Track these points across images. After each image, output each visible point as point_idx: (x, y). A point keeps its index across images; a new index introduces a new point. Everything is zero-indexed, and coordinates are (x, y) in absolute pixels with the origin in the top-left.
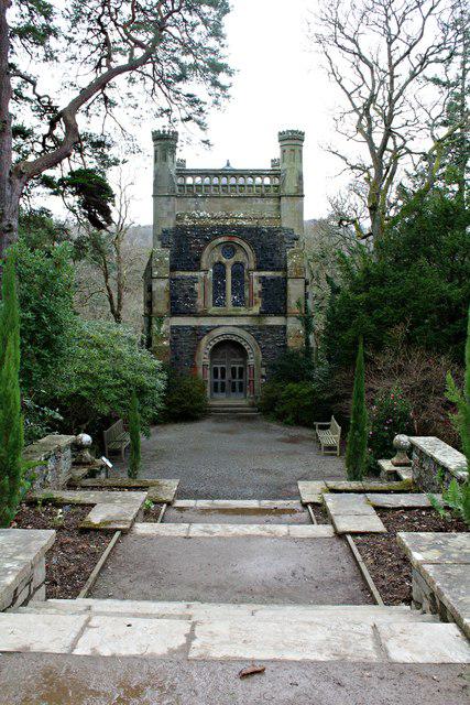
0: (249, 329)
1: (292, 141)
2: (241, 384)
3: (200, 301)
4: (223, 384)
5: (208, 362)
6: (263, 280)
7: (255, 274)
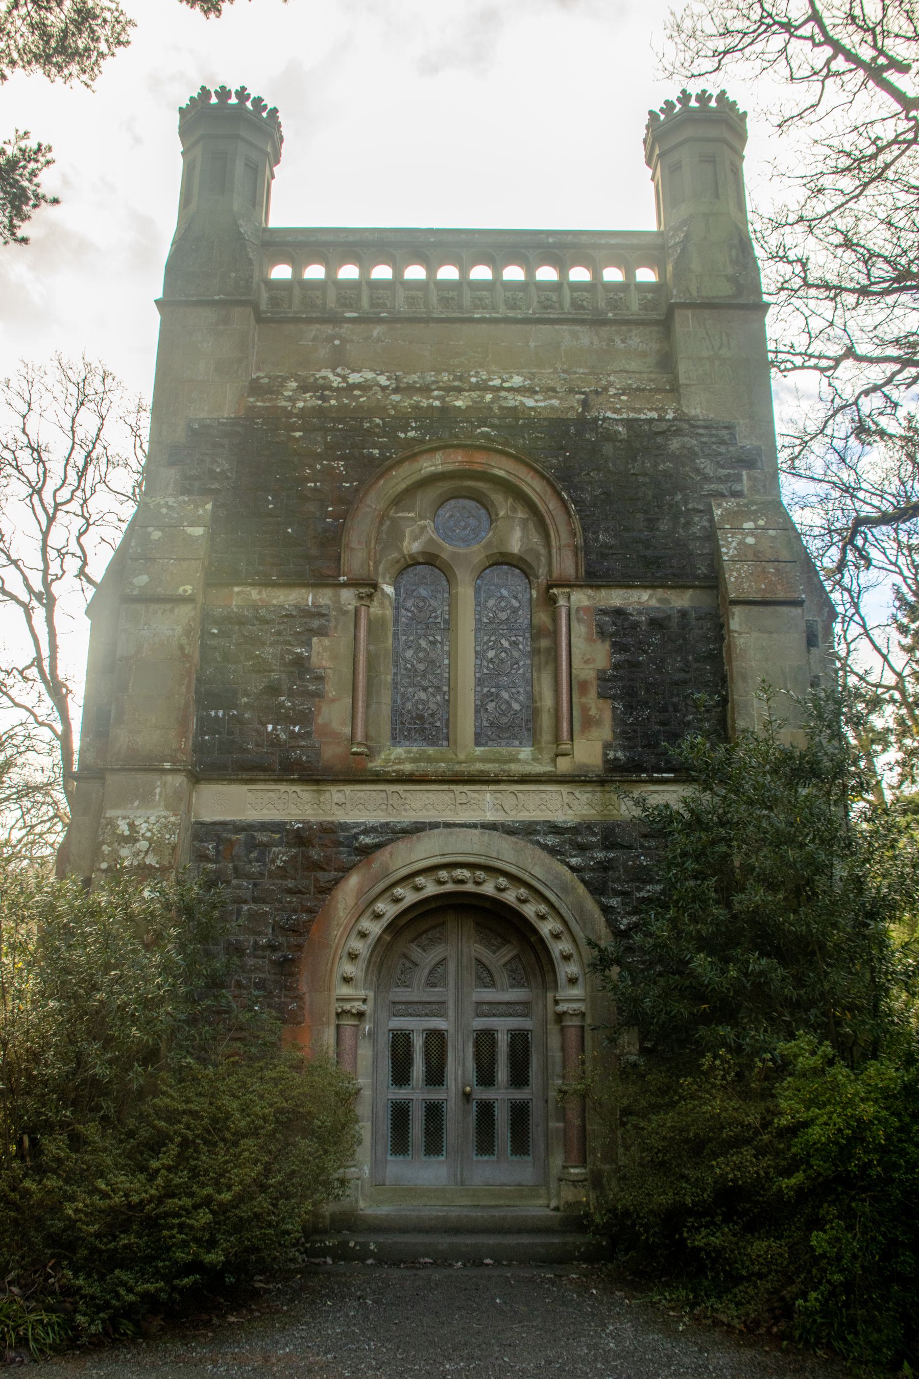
0: (563, 839)
1: (697, 142)
2: (520, 1113)
3: (334, 715)
4: (434, 1111)
7: (581, 598)
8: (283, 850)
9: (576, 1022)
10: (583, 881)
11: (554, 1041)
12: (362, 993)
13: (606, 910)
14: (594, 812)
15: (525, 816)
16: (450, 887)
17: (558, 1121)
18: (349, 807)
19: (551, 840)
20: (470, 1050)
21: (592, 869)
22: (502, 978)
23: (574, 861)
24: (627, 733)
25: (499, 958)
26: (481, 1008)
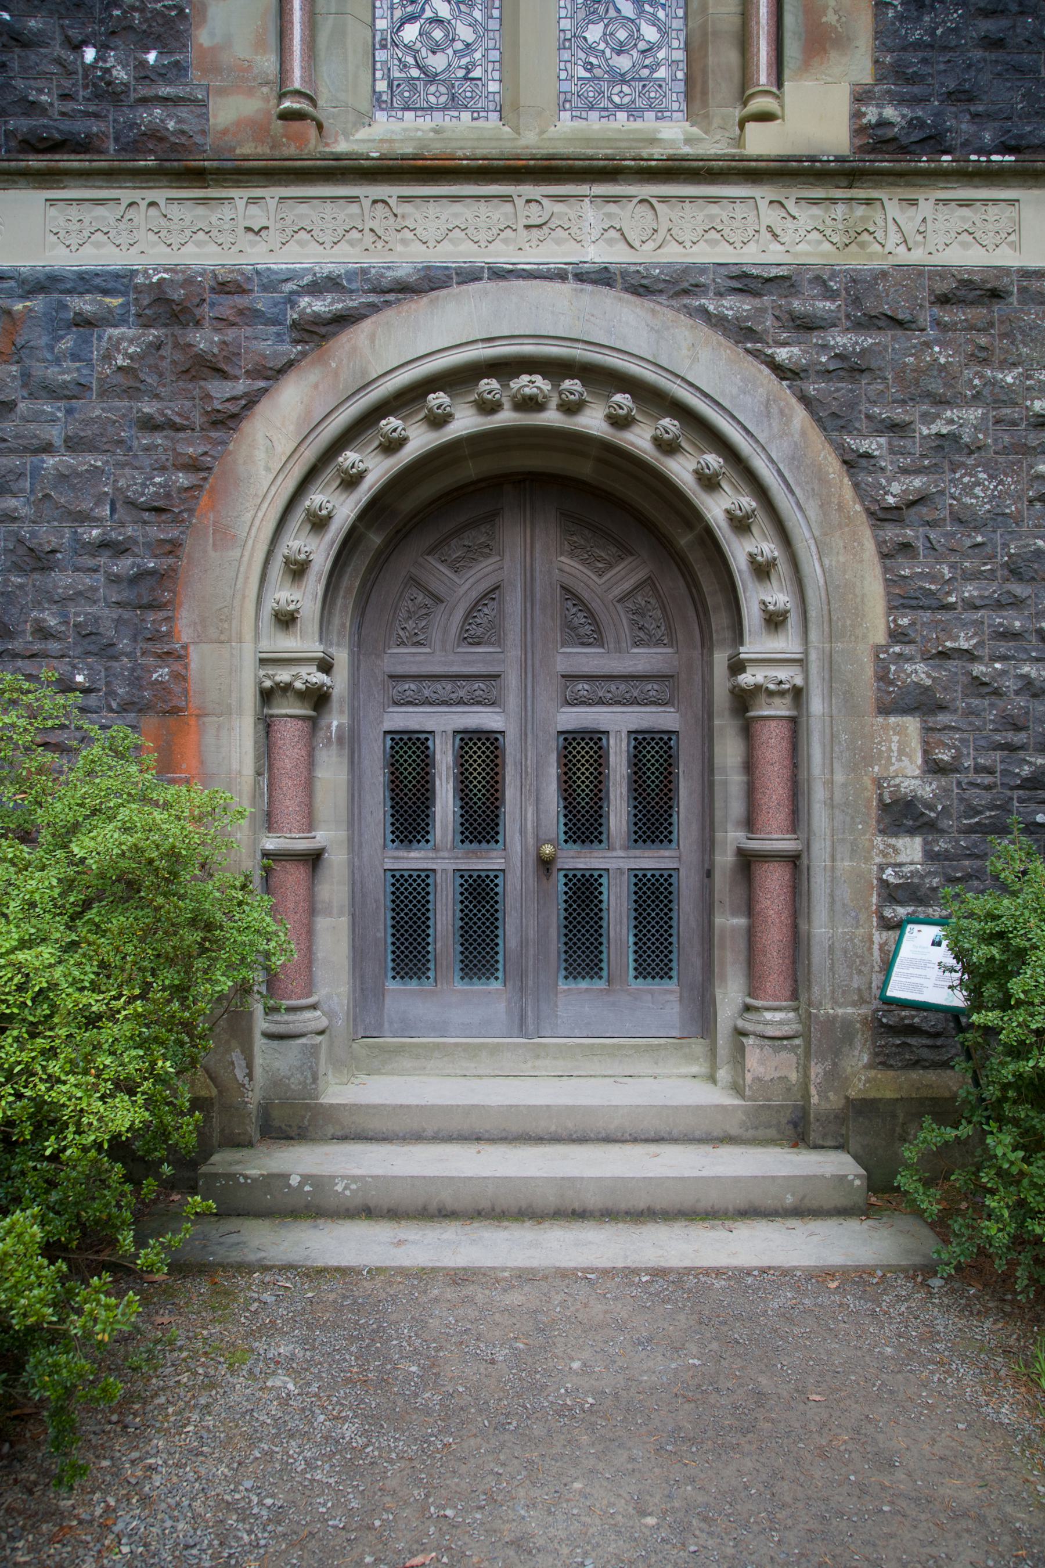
2: (653, 895)
4: (480, 894)
8: (130, 332)
9: (781, 708)
10: (804, 399)
11: (729, 751)
12: (314, 648)
13: (853, 462)
14: (827, 246)
15: (673, 254)
16: (506, 417)
17: (734, 913)
18: (274, 237)
19: (732, 306)
20: (552, 771)
21: (826, 373)
22: (618, 622)
23: (782, 354)
25: (611, 581)
26: (578, 688)
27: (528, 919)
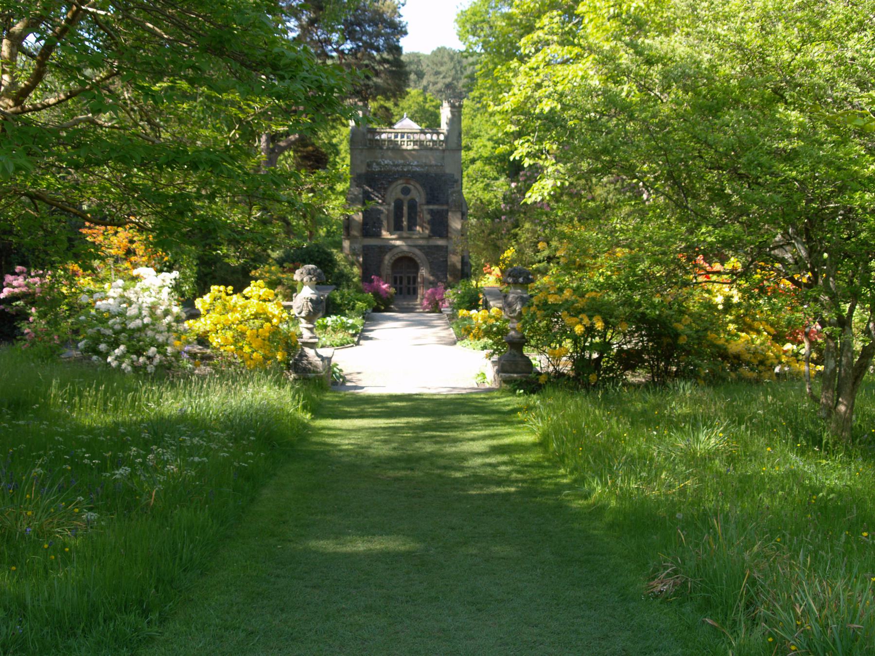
0: (421, 248)
5: (390, 272)
6: (431, 212)
7: (425, 207)
24: (432, 231)
27: (405, 290)
